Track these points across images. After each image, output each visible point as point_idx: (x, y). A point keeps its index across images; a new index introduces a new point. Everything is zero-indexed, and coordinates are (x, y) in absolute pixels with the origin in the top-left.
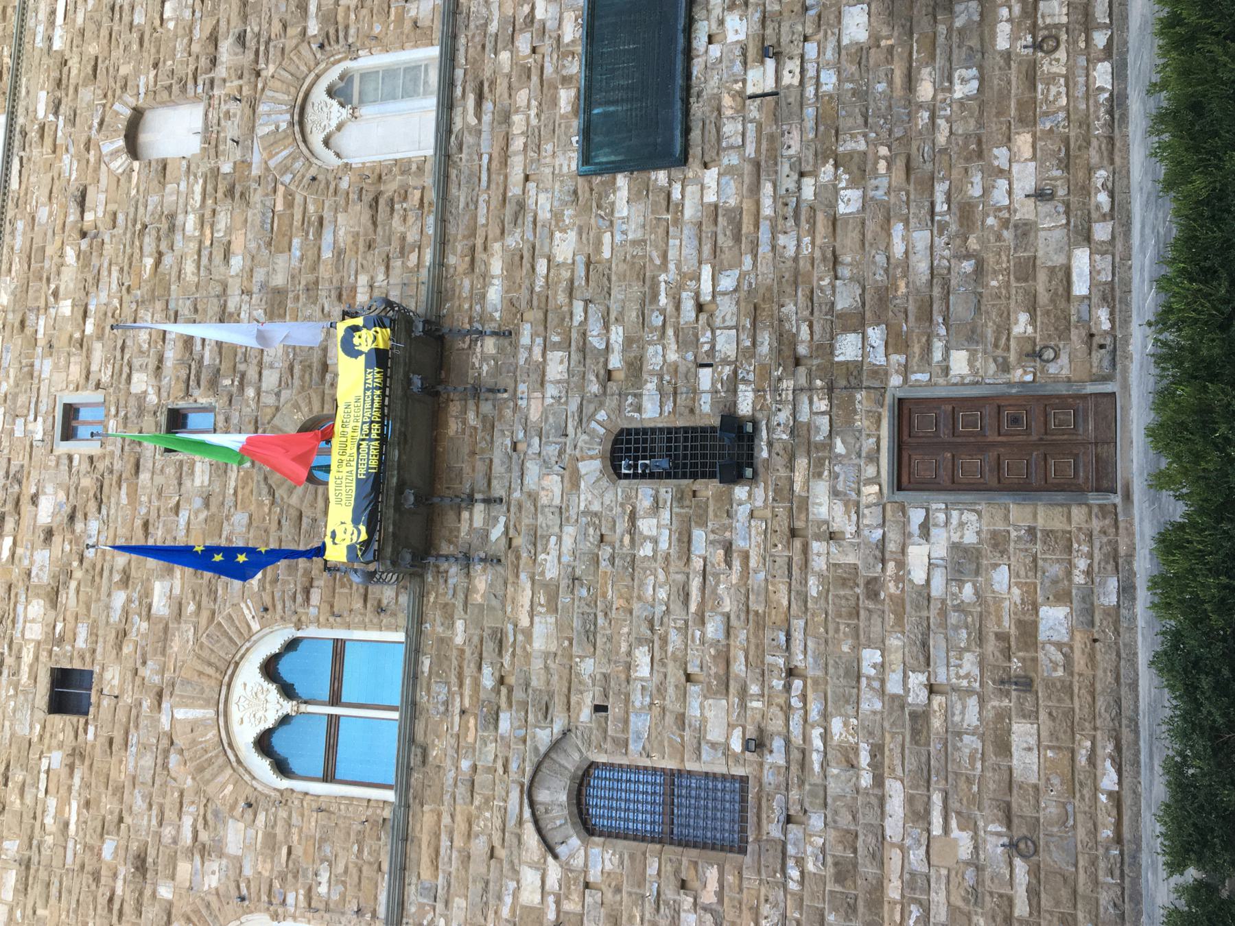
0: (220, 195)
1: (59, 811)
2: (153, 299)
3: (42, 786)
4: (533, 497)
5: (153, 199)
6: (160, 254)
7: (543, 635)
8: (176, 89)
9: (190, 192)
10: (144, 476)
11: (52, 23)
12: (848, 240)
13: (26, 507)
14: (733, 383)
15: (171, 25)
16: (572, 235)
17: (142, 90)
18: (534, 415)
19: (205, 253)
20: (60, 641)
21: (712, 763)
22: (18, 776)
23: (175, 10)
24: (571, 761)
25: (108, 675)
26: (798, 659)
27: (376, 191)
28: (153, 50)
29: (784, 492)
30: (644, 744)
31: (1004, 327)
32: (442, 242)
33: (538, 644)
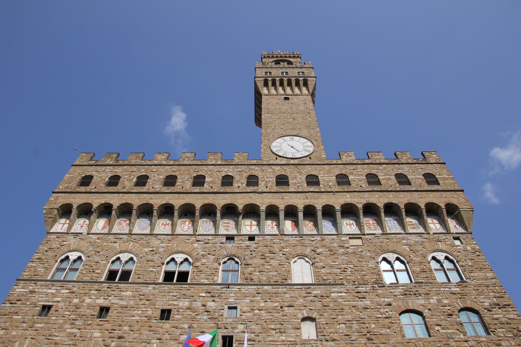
1: (137, 314)
2: (262, 329)
3: (144, 309)
6: (275, 330)
9: (291, 337)
11: (338, 292)
15: (338, 327)
17: (320, 320)
19: (274, 343)
20: (178, 311)
22: (148, 303)
23: (342, 327)
25: (168, 324)
28: (331, 322)
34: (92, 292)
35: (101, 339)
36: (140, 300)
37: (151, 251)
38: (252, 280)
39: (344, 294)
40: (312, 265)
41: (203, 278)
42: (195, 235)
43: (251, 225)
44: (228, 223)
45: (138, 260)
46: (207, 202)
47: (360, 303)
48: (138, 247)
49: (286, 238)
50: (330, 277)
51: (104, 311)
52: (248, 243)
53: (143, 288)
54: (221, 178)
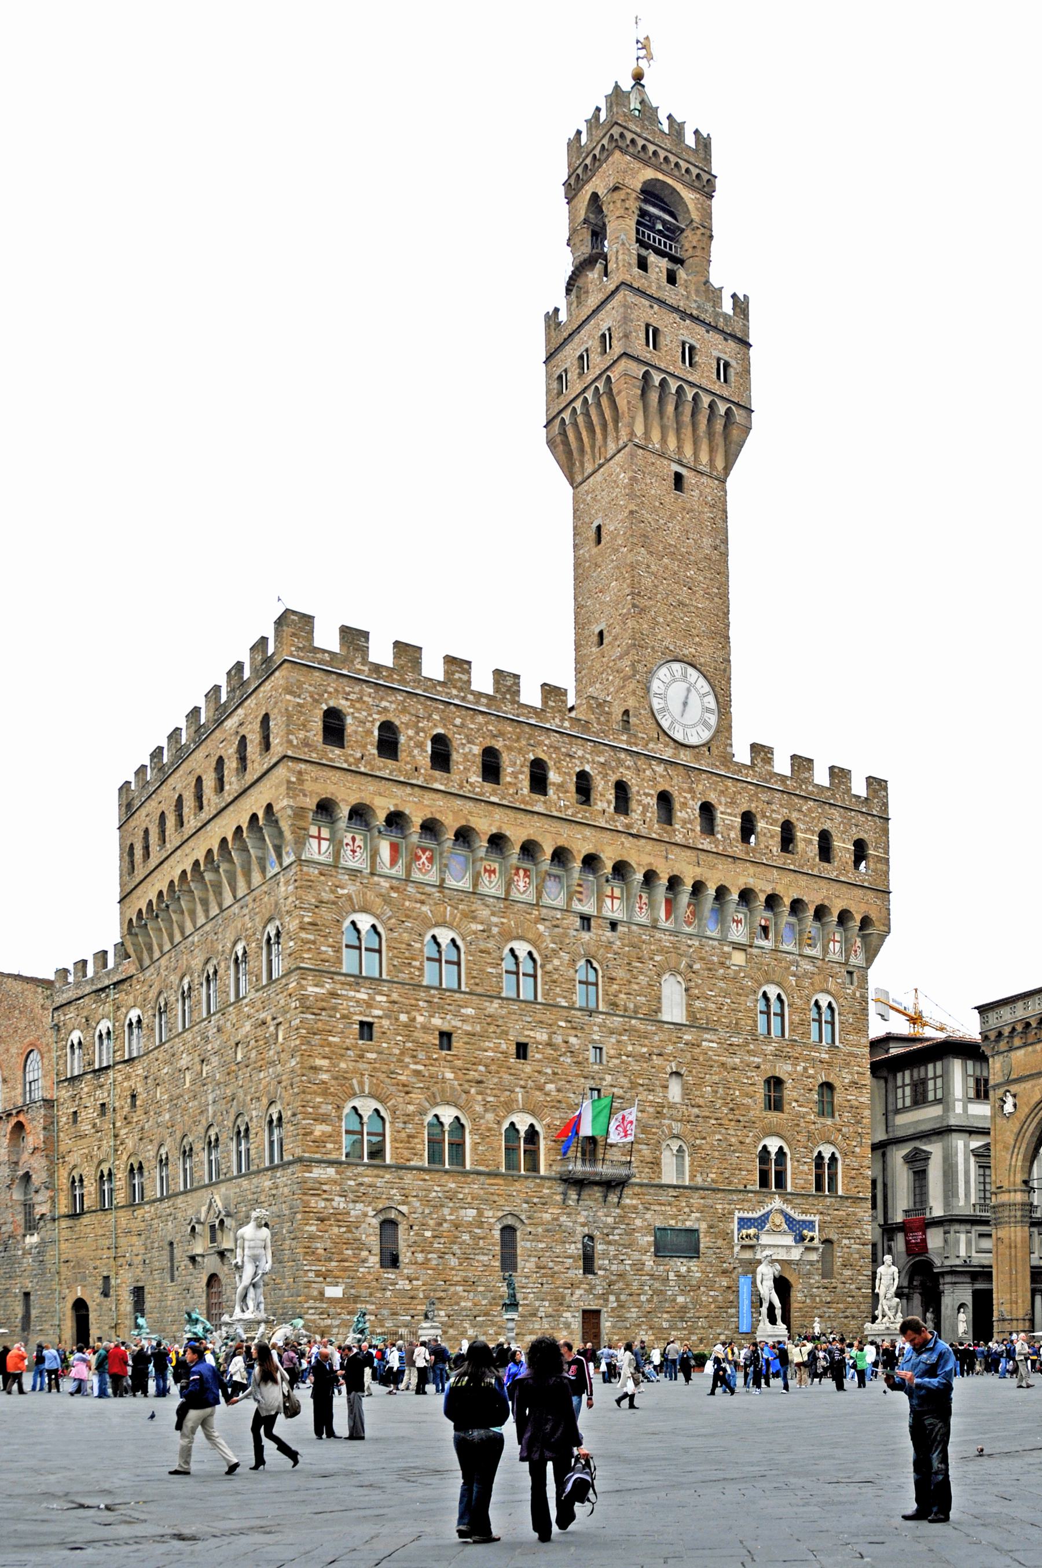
0: (659, 1109)
1: (490, 1048)
4: (579, 1214)
5: (657, 1083)
6: (642, 1085)
7: (547, 1217)
8: (686, 1092)
10: (583, 1080)
12: (635, 1298)
13: (573, 1032)
14: (606, 1270)
16: (640, 1224)
18: (599, 1214)
21: (520, 1264)
24: (518, 1225)
26: (545, 1286)
27: (655, 1164)
29: (581, 1283)
30: (522, 1245)
31: (615, 1334)
32: (641, 1185)
33: (545, 1215)
34: (421, 1003)
35: (456, 1083)
36: (488, 1024)
37: (483, 931)
38: (615, 1005)
39: (715, 1045)
40: (687, 990)
41: (560, 996)
42: (537, 904)
43: (612, 897)
44: (580, 885)
45: (466, 946)
46: (561, 842)
47: (729, 1060)
48: (461, 919)
49: (658, 935)
50: (702, 1015)
51: (446, 1038)
52: (609, 934)
53: (487, 1004)
54: (575, 779)
